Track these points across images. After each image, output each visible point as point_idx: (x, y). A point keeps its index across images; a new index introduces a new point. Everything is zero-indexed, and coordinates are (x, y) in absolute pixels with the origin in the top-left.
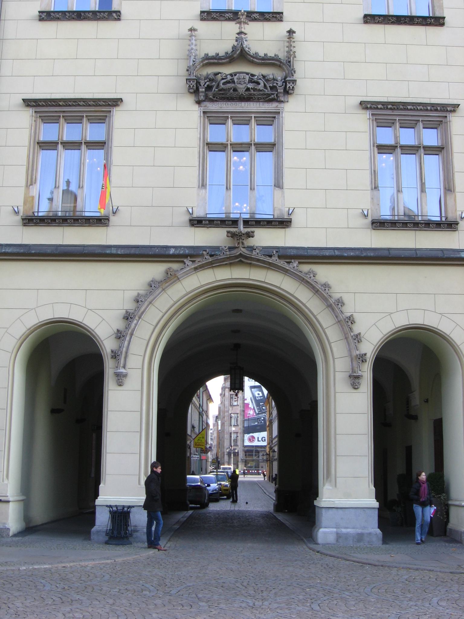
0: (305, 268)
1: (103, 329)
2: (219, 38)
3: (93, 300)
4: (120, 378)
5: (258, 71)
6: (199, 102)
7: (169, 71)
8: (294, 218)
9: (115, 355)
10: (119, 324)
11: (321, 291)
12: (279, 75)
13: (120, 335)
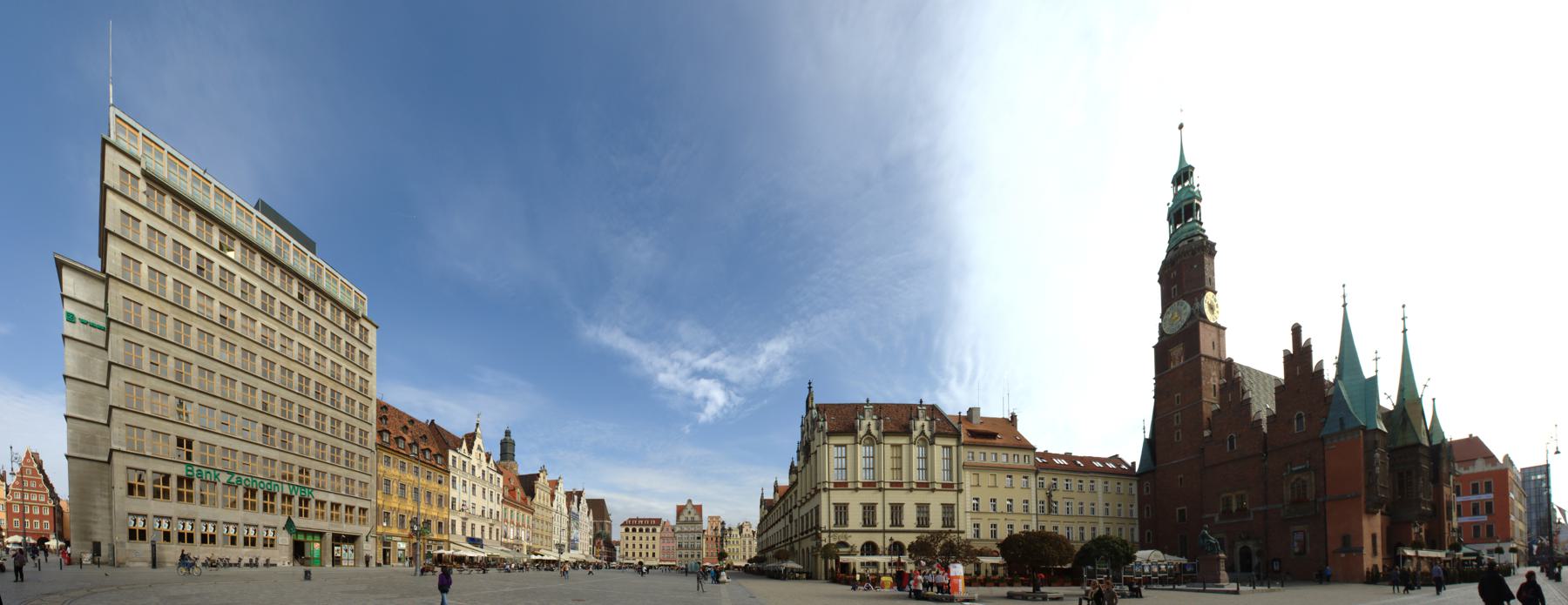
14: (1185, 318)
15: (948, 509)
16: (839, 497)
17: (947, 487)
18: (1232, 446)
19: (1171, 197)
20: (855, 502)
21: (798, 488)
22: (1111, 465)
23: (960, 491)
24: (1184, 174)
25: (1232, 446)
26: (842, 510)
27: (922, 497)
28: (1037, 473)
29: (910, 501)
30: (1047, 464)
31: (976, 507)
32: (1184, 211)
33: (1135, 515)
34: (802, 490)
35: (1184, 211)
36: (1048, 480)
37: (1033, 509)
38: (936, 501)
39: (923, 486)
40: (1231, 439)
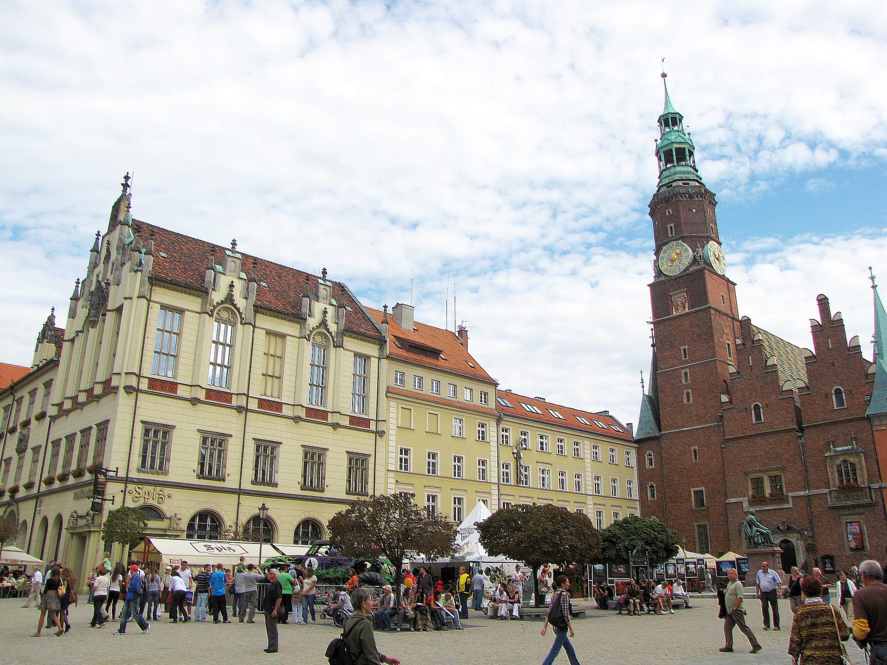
15: (358, 463)
16: (156, 409)
17: (359, 423)
18: (758, 417)
20: (188, 426)
21: (59, 376)
22: (601, 424)
23: (380, 434)
25: (758, 417)
26: (157, 436)
27: (316, 435)
28: (499, 420)
29: (292, 438)
30: (513, 410)
31: (404, 464)
33: (636, 495)
34: (65, 383)
36: (514, 433)
37: (493, 475)
38: (338, 446)
39: (317, 415)
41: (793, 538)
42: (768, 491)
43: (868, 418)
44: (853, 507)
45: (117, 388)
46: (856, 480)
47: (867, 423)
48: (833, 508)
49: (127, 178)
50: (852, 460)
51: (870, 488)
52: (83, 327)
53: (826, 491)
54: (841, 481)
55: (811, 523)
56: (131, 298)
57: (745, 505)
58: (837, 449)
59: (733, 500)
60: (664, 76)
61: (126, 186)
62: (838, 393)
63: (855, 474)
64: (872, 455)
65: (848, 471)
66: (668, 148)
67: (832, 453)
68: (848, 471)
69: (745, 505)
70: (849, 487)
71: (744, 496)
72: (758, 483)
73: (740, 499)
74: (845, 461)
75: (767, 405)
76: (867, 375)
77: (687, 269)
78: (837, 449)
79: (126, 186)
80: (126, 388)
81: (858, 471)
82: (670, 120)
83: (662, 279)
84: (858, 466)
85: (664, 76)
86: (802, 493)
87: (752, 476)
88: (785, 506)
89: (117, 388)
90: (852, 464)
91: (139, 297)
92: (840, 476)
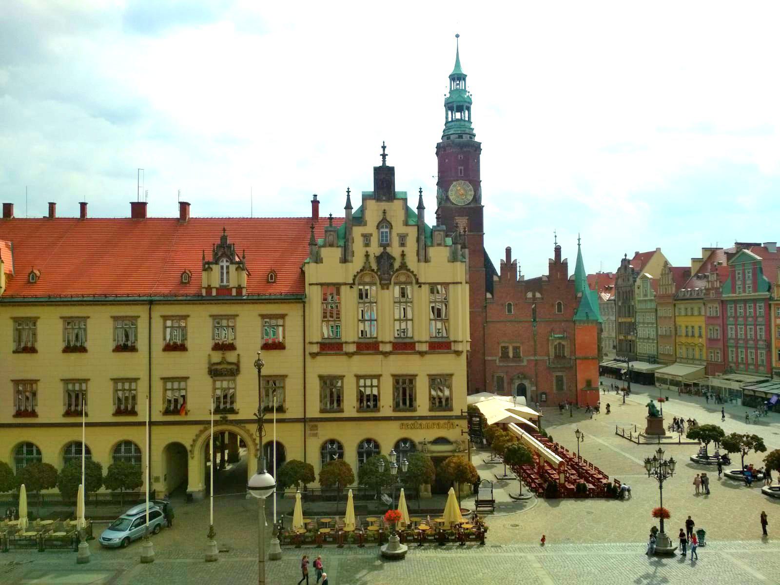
0: (243, 425)
1: (187, 444)
2: (217, 357)
3: (185, 436)
4: (192, 458)
5: (230, 367)
6: (212, 377)
7: (205, 367)
8: (239, 411)
9: (190, 451)
10: (191, 443)
11: (248, 431)
12: (235, 367)
13: (192, 446)
14: (471, 198)
18: (509, 311)
19: (447, 92)
24: (457, 77)
25: (509, 311)
32: (458, 104)
35: (458, 104)
40: (509, 305)
41: (527, 383)
42: (511, 355)
43: (574, 322)
44: (561, 368)
45: (462, 352)
46: (564, 353)
47: (573, 324)
48: (549, 368)
49: (384, 147)
50: (563, 343)
51: (570, 359)
52: (354, 280)
53: (547, 358)
54: (555, 353)
55: (536, 375)
56: (461, 283)
57: (497, 361)
58: (556, 336)
59: (489, 358)
60: (457, 36)
61: (384, 156)
62: (559, 304)
63: (563, 350)
64: (573, 341)
65: (561, 347)
66: (461, 104)
67: (553, 338)
68: (561, 347)
69: (497, 361)
70: (559, 357)
71: (496, 356)
72: (505, 349)
73: (494, 358)
74: (559, 344)
75: (516, 304)
76: (576, 297)
77: (469, 204)
78: (556, 336)
79: (384, 156)
80: (468, 351)
81: (566, 349)
82: (457, 77)
83: (449, 205)
84: (566, 347)
85: (457, 36)
86: (532, 358)
87: (503, 345)
88: (523, 364)
89: (462, 352)
90: (563, 346)
91: (466, 283)
92: (555, 350)
